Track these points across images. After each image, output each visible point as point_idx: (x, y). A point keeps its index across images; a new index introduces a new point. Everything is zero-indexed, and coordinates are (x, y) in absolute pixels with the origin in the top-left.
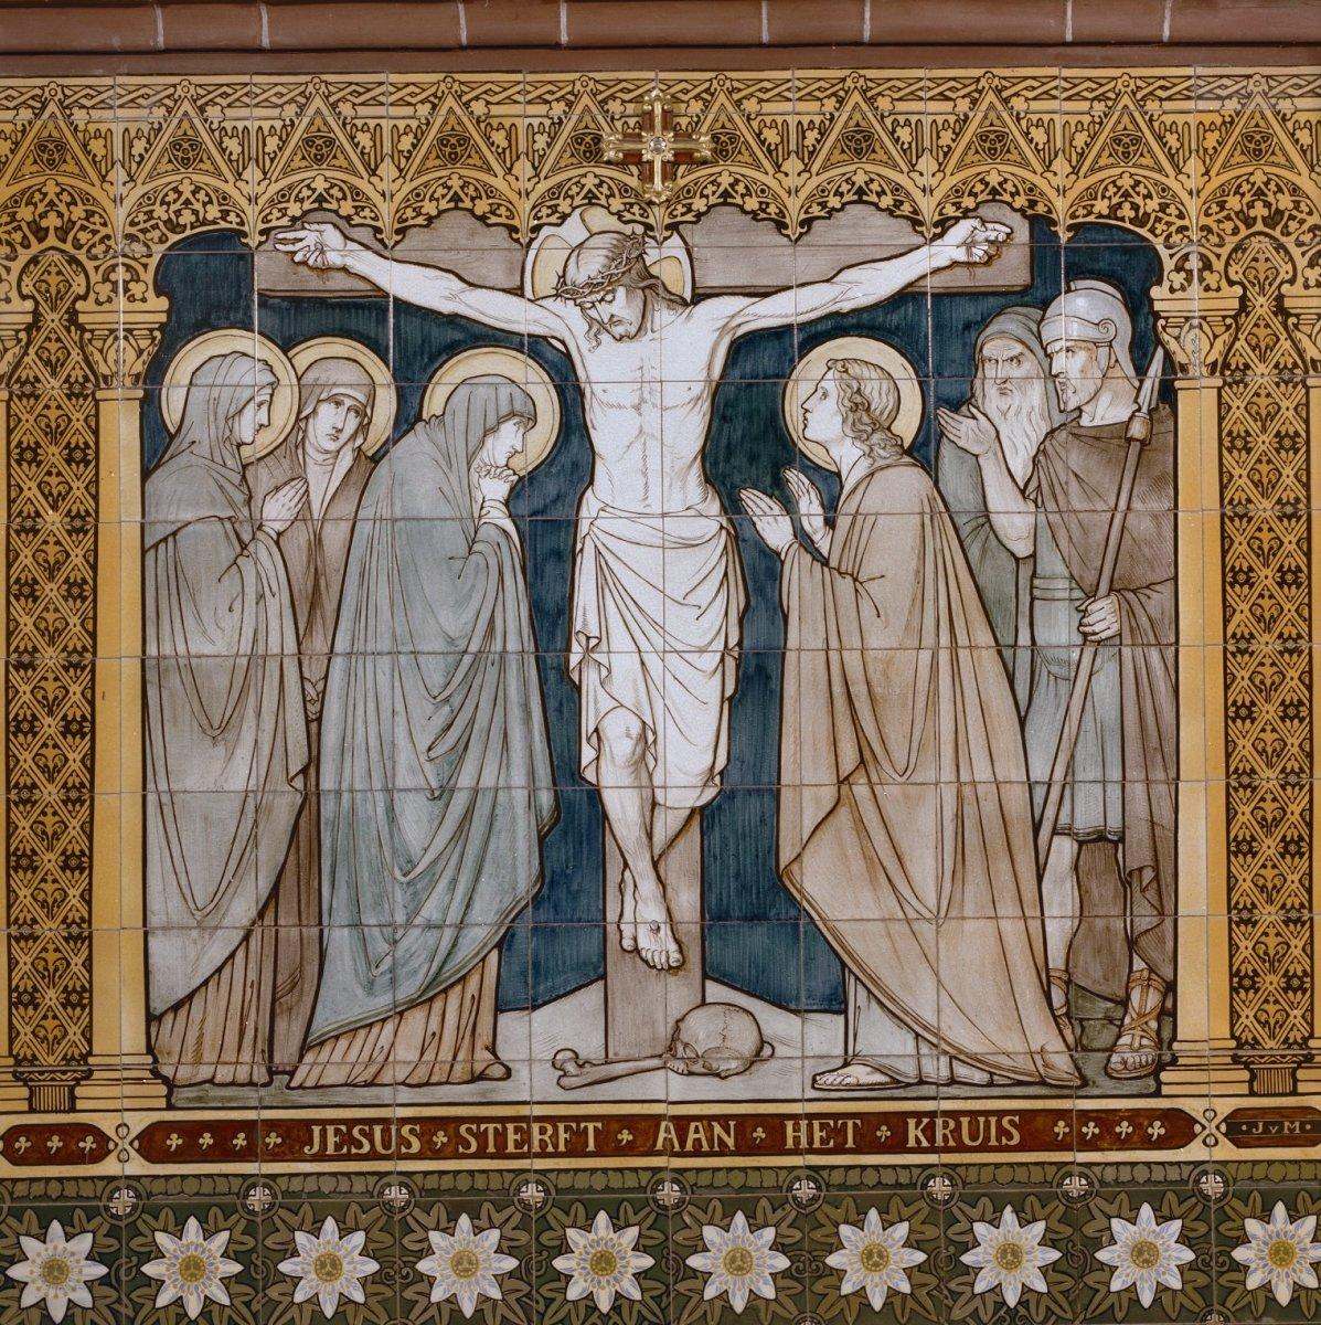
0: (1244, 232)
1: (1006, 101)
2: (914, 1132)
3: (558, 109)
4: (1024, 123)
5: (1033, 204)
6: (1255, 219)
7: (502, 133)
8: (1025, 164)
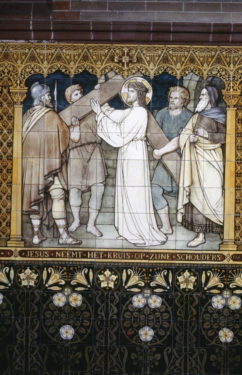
0: (3, 76)
1: (35, 50)
2: (109, 256)
3: (27, 51)
4: (171, 56)
5: (146, 72)
6: (5, 73)
7: (16, 55)
8: (145, 64)
